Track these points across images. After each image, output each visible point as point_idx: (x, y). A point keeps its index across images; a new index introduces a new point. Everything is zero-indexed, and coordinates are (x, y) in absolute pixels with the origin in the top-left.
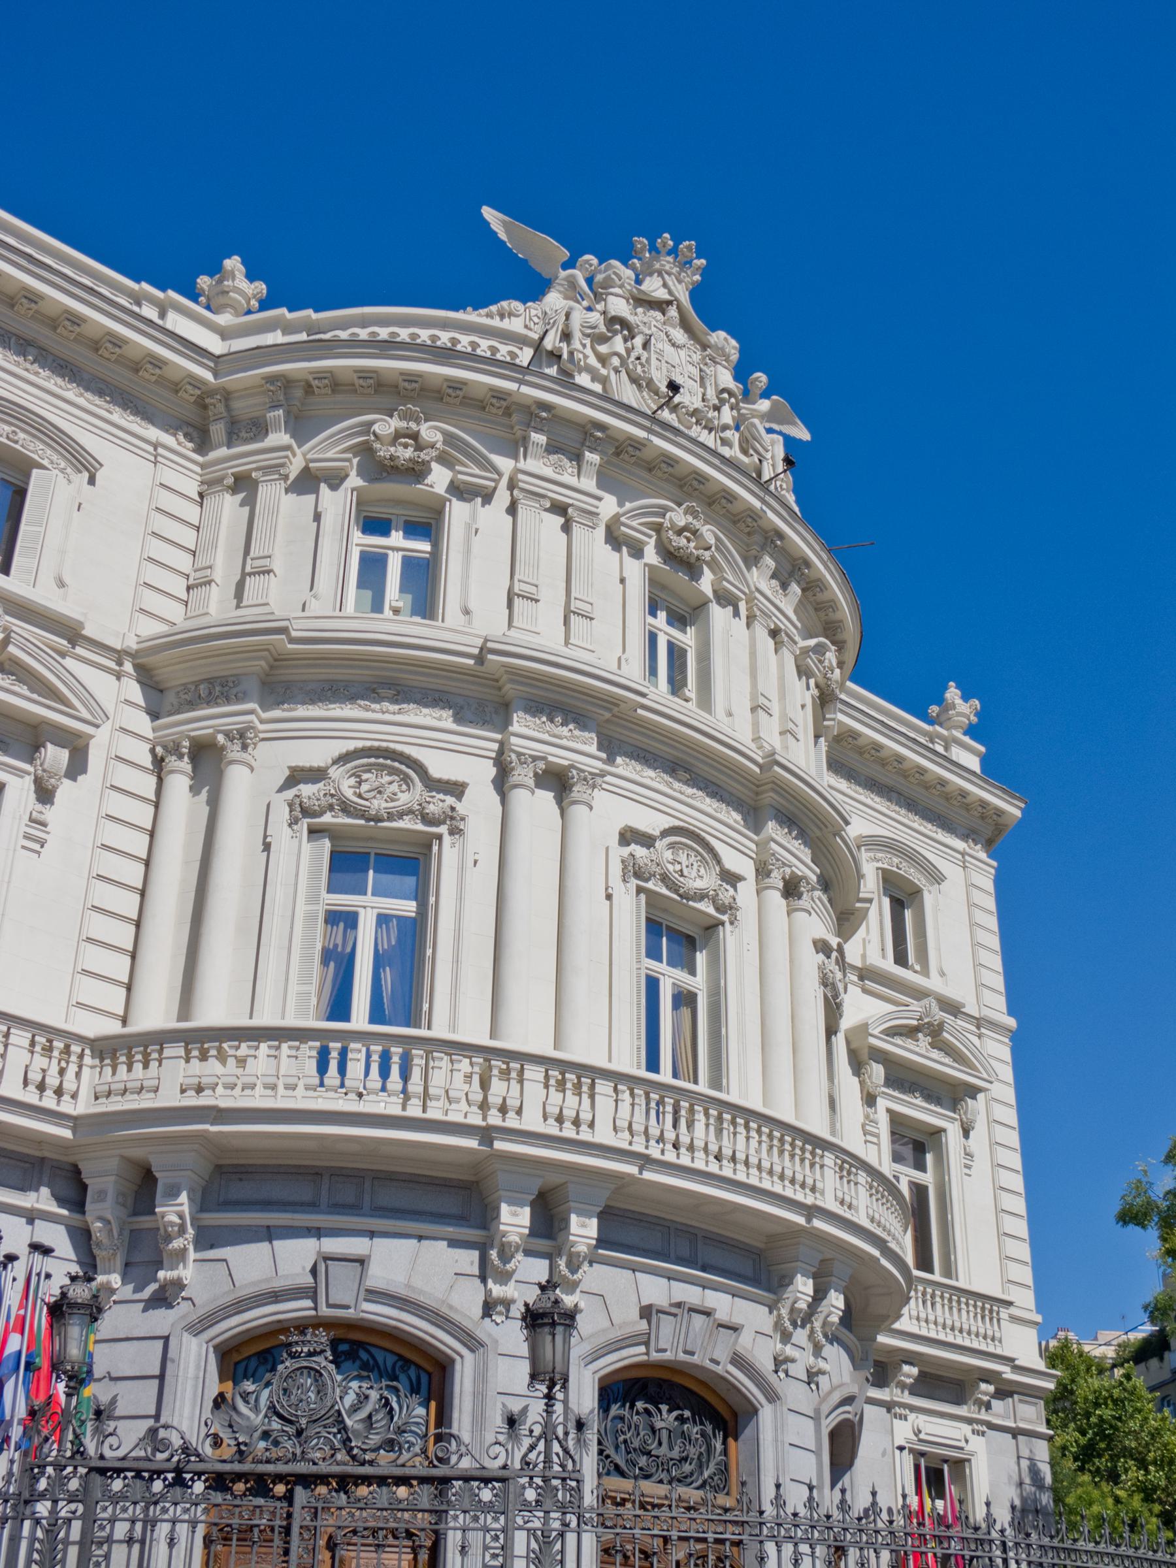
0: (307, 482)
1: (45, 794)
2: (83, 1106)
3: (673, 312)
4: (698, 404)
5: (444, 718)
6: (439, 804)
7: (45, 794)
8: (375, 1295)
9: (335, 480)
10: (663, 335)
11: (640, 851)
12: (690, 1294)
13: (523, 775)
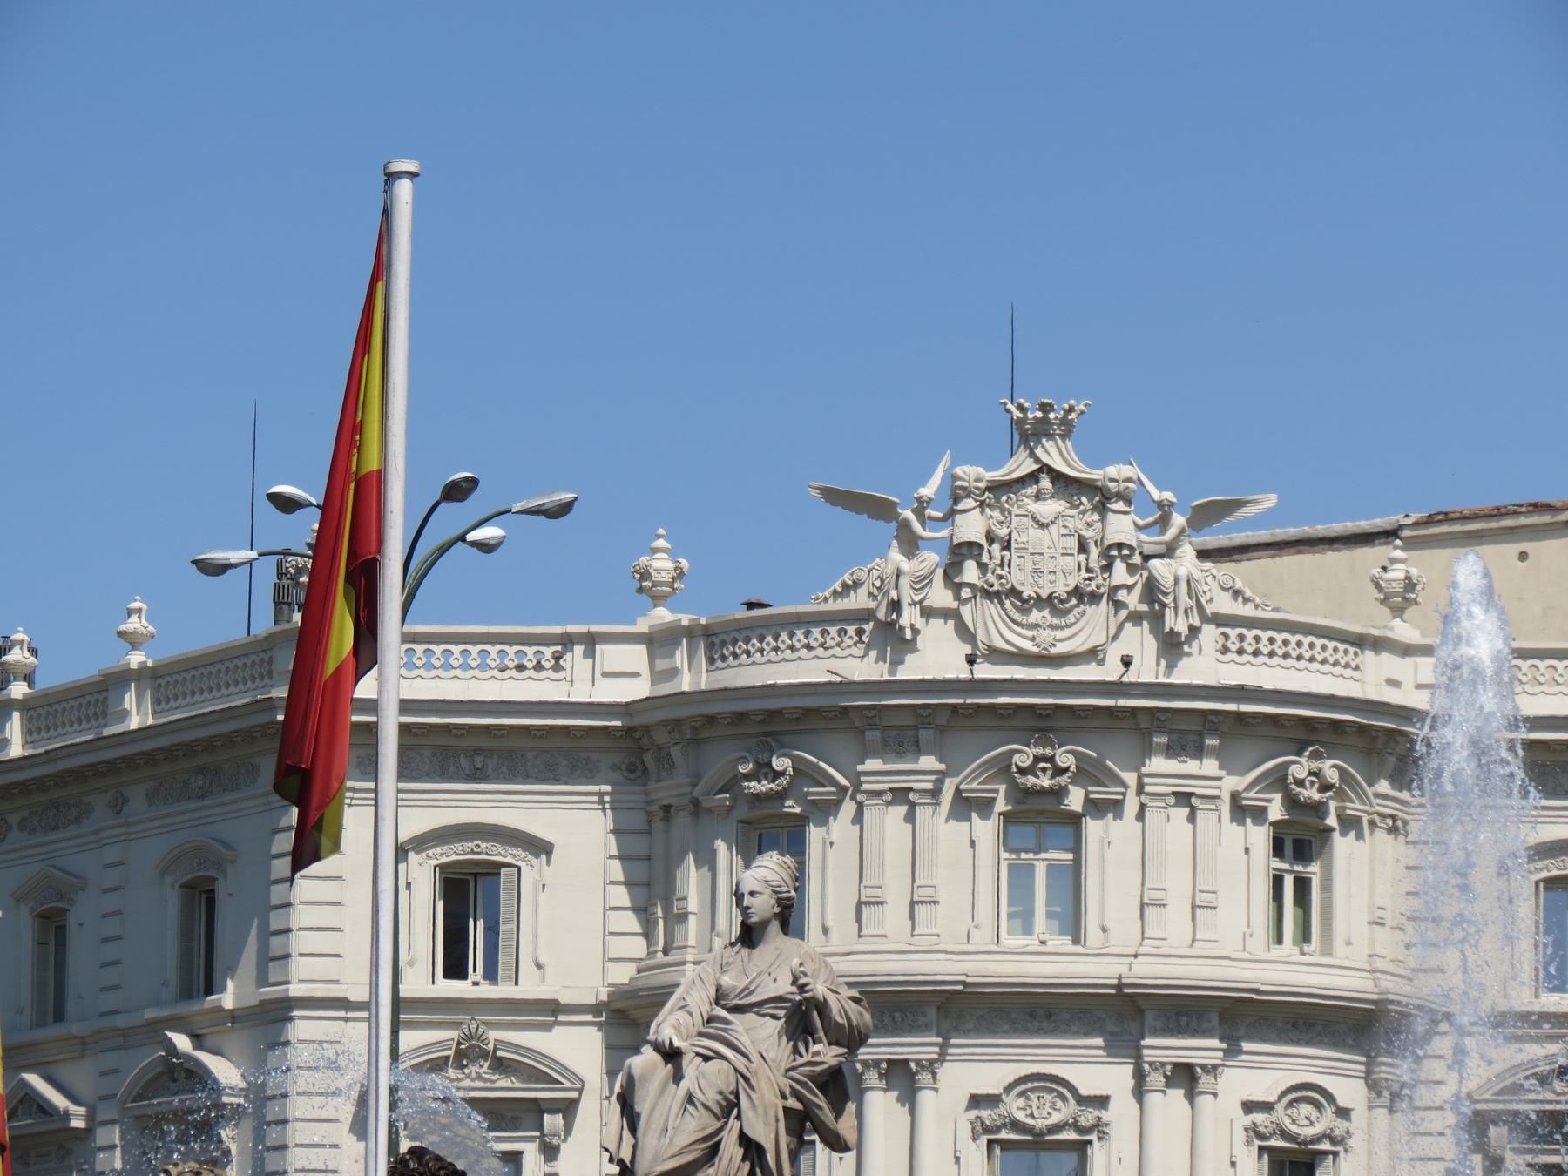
3: (1045, 483)
10: (1028, 522)
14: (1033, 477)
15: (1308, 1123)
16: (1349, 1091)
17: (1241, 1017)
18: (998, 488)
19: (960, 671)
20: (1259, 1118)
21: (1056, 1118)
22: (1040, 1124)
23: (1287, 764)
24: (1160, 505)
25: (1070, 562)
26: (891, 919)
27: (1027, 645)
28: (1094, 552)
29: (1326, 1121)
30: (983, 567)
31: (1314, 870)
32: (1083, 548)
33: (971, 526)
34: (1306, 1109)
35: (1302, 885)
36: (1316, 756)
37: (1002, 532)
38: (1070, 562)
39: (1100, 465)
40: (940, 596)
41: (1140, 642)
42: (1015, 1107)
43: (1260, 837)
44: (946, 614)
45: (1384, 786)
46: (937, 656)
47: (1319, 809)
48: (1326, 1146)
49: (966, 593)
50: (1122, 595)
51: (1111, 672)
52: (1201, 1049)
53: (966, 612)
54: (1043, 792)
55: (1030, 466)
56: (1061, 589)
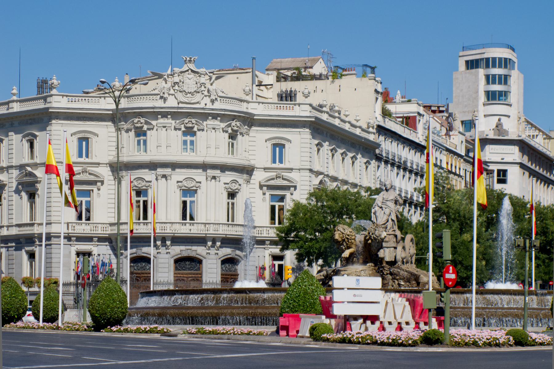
0: (128, 131)
1: (99, 190)
2: (109, 232)
3: (190, 71)
4: (195, 89)
5: (147, 170)
6: (147, 184)
7: (99, 190)
8: (143, 253)
9: (131, 130)
11: (180, 184)
12: (187, 247)
13: (159, 178)
14: (188, 71)
15: (234, 187)
16: (241, 181)
17: (224, 168)
18: (182, 72)
19: (176, 105)
20: (227, 185)
21: (192, 185)
22: (189, 186)
23: (231, 123)
24: (209, 76)
25: (194, 86)
26: (163, 149)
27: (187, 101)
28: (198, 84)
29: (237, 186)
30: (179, 87)
31: (235, 142)
32: (196, 84)
33: (176, 79)
34: (234, 184)
35: (233, 144)
36: (236, 121)
37: (182, 80)
38: (194, 86)
39: (199, 69)
40: (172, 92)
41: (207, 100)
42: (185, 183)
43: (227, 135)
44: (172, 95)
45: (246, 127)
46: (172, 102)
47: (237, 131)
48: (237, 191)
49: (176, 91)
50: (203, 92)
51: (202, 105)
52: (217, 173)
53: (176, 94)
54: (190, 127)
55: (187, 69)
56: (193, 91)
